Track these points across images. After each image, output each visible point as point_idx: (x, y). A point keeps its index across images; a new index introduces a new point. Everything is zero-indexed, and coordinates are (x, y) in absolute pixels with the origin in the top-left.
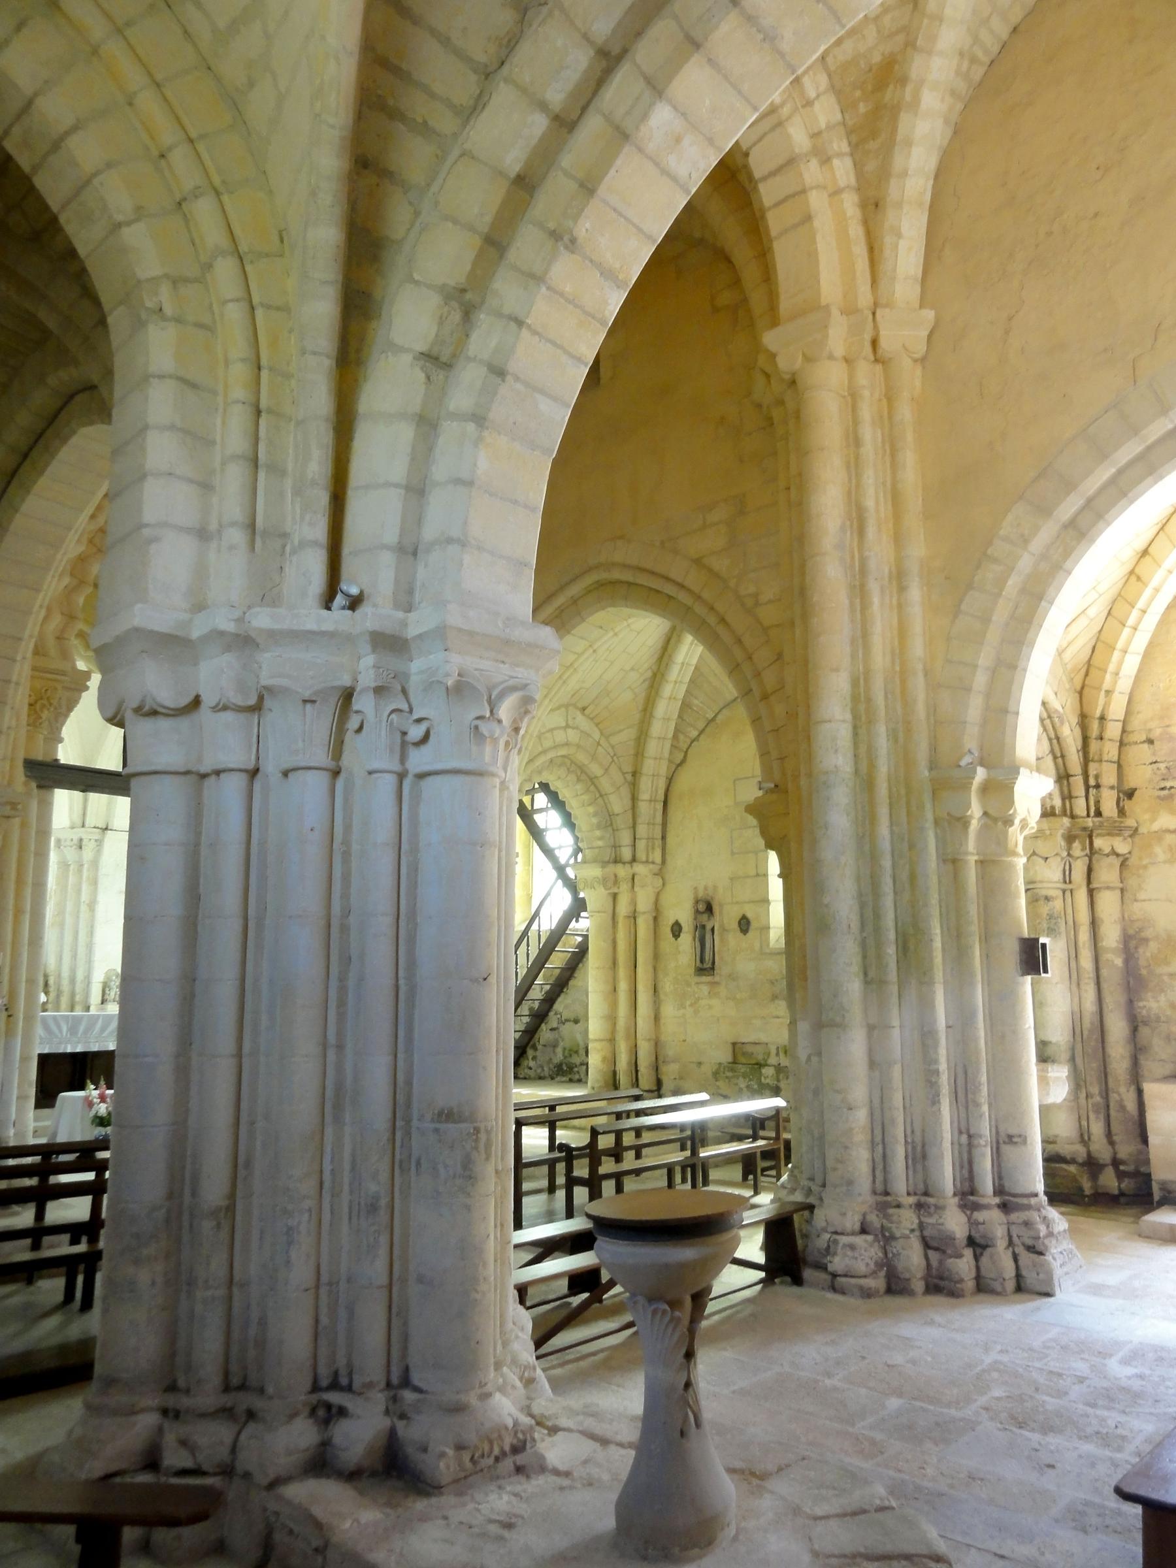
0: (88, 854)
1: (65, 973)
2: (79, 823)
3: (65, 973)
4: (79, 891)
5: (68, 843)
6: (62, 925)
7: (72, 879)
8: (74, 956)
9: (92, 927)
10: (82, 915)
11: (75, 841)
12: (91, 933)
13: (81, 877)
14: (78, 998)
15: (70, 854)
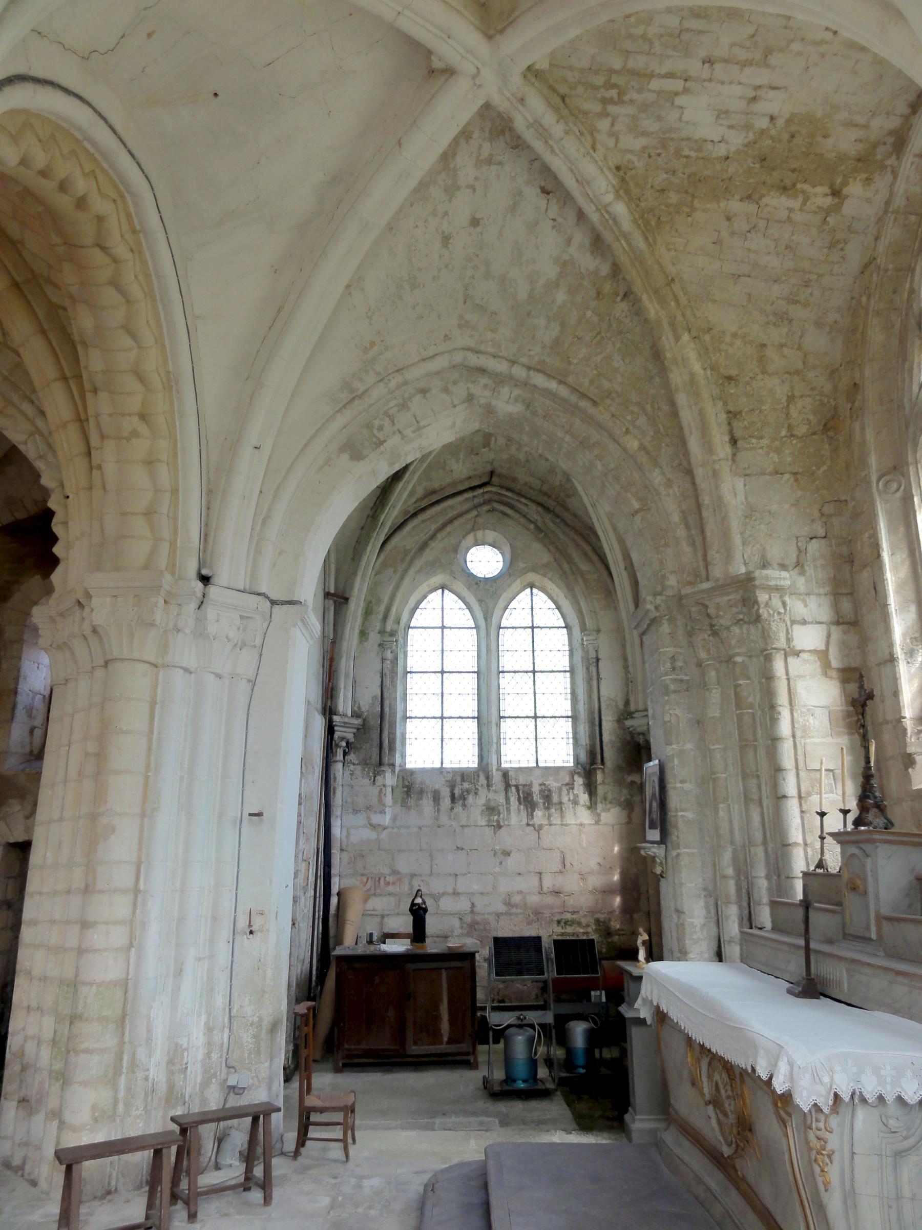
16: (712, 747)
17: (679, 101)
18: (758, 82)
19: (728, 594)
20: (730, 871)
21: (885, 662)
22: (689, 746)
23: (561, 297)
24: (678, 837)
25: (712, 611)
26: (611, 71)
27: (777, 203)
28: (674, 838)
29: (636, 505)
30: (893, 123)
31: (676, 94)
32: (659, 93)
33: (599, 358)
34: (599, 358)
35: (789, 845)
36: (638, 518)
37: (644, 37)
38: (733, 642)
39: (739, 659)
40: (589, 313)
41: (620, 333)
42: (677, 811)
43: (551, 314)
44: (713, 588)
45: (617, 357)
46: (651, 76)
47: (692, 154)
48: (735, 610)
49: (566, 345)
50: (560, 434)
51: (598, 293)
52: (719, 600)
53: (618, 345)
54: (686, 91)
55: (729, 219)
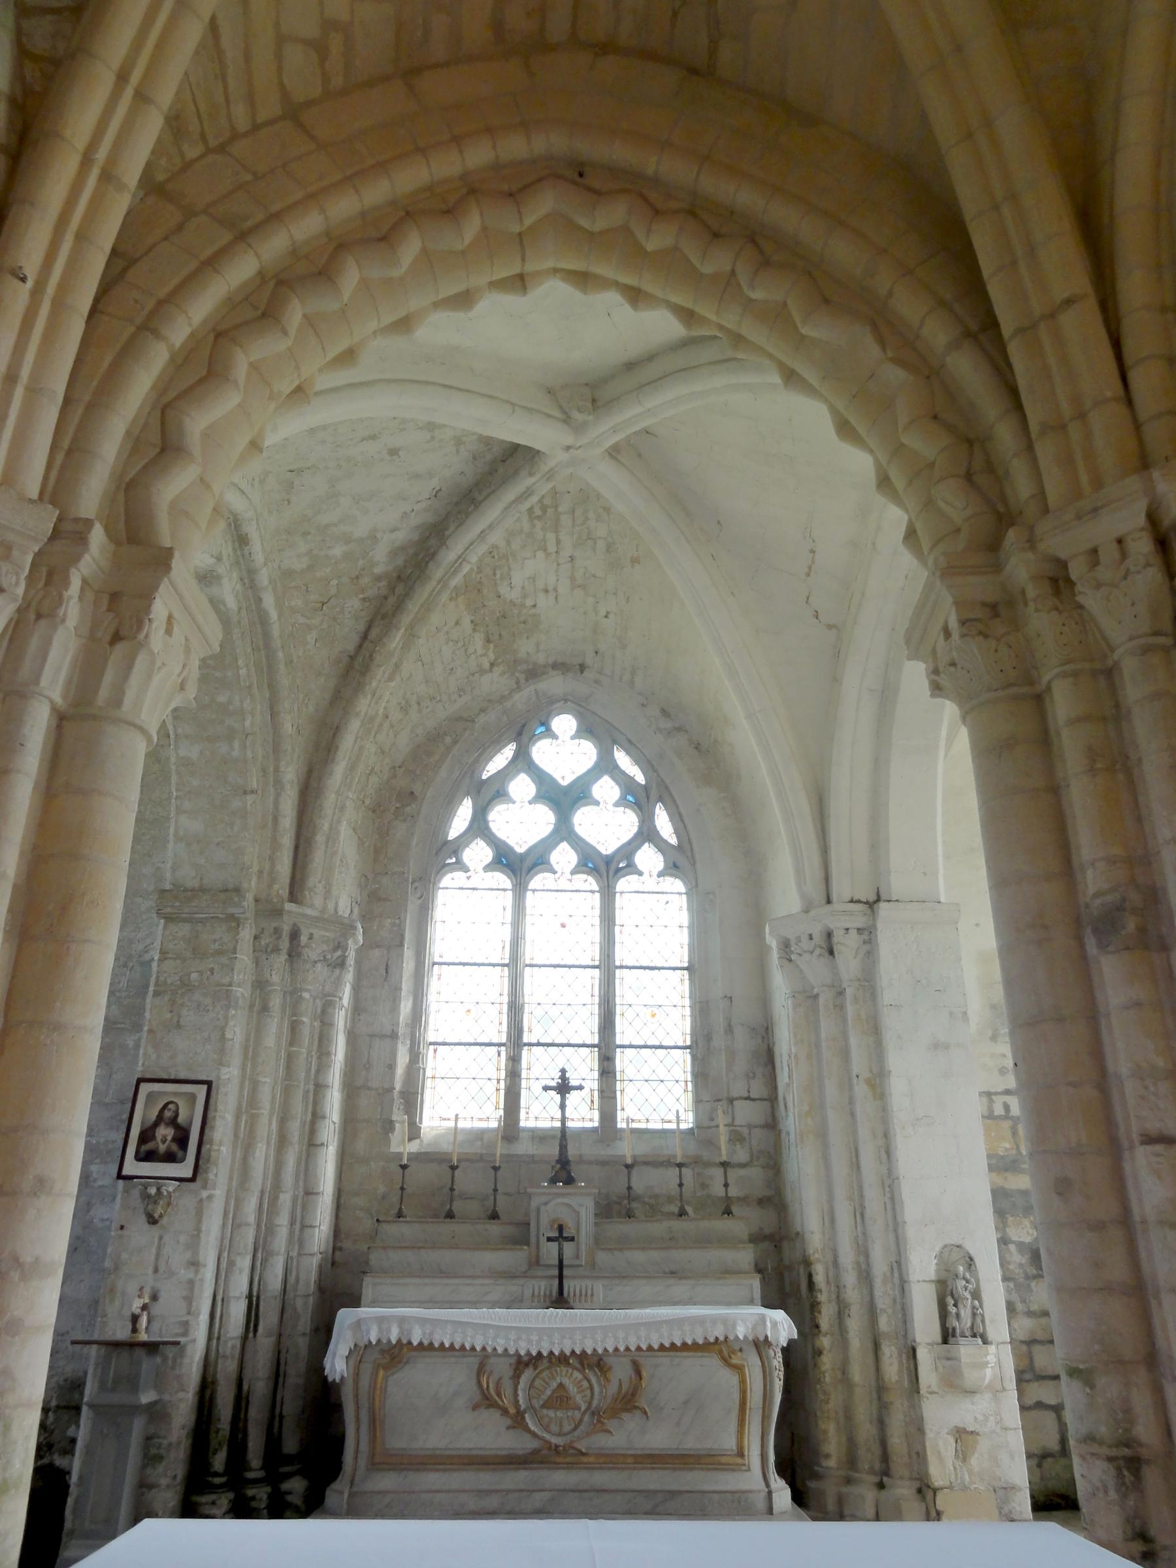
0: (849, 961)
1: (847, 1257)
2: (820, 897)
3: (847, 1257)
4: (845, 1054)
5: (806, 944)
6: (822, 1135)
7: (827, 1026)
8: (860, 1213)
9: (886, 1135)
10: (859, 1110)
11: (819, 939)
12: (888, 1152)
13: (844, 1020)
14: (884, 1323)
15: (815, 969)
16: (263, 1080)
17: (540, 554)
18: (560, 590)
19: (327, 930)
20: (252, 1219)
21: (383, 1037)
22: (236, 1073)
23: (337, 551)
24: (216, 1175)
25: (304, 939)
26: (556, 507)
27: (478, 641)
28: (211, 1176)
29: (254, 783)
30: (541, 659)
31: (545, 550)
32: (544, 540)
33: (302, 620)
34: (302, 620)
35: (318, 1194)
36: (250, 799)
37: (587, 519)
38: (311, 977)
39: (306, 995)
40: (334, 582)
41: (335, 619)
42: (220, 1145)
43: (315, 552)
44: (317, 918)
45: (314, 634)
46: (557, 532)
47: (498, 576)
48: (325, 947)
49: (293, 584)
50: (240, 662)
51: (357, 577)
52: (314, 931)
53: (325, 626)
54: (548, 555)
55: (457, 623)
